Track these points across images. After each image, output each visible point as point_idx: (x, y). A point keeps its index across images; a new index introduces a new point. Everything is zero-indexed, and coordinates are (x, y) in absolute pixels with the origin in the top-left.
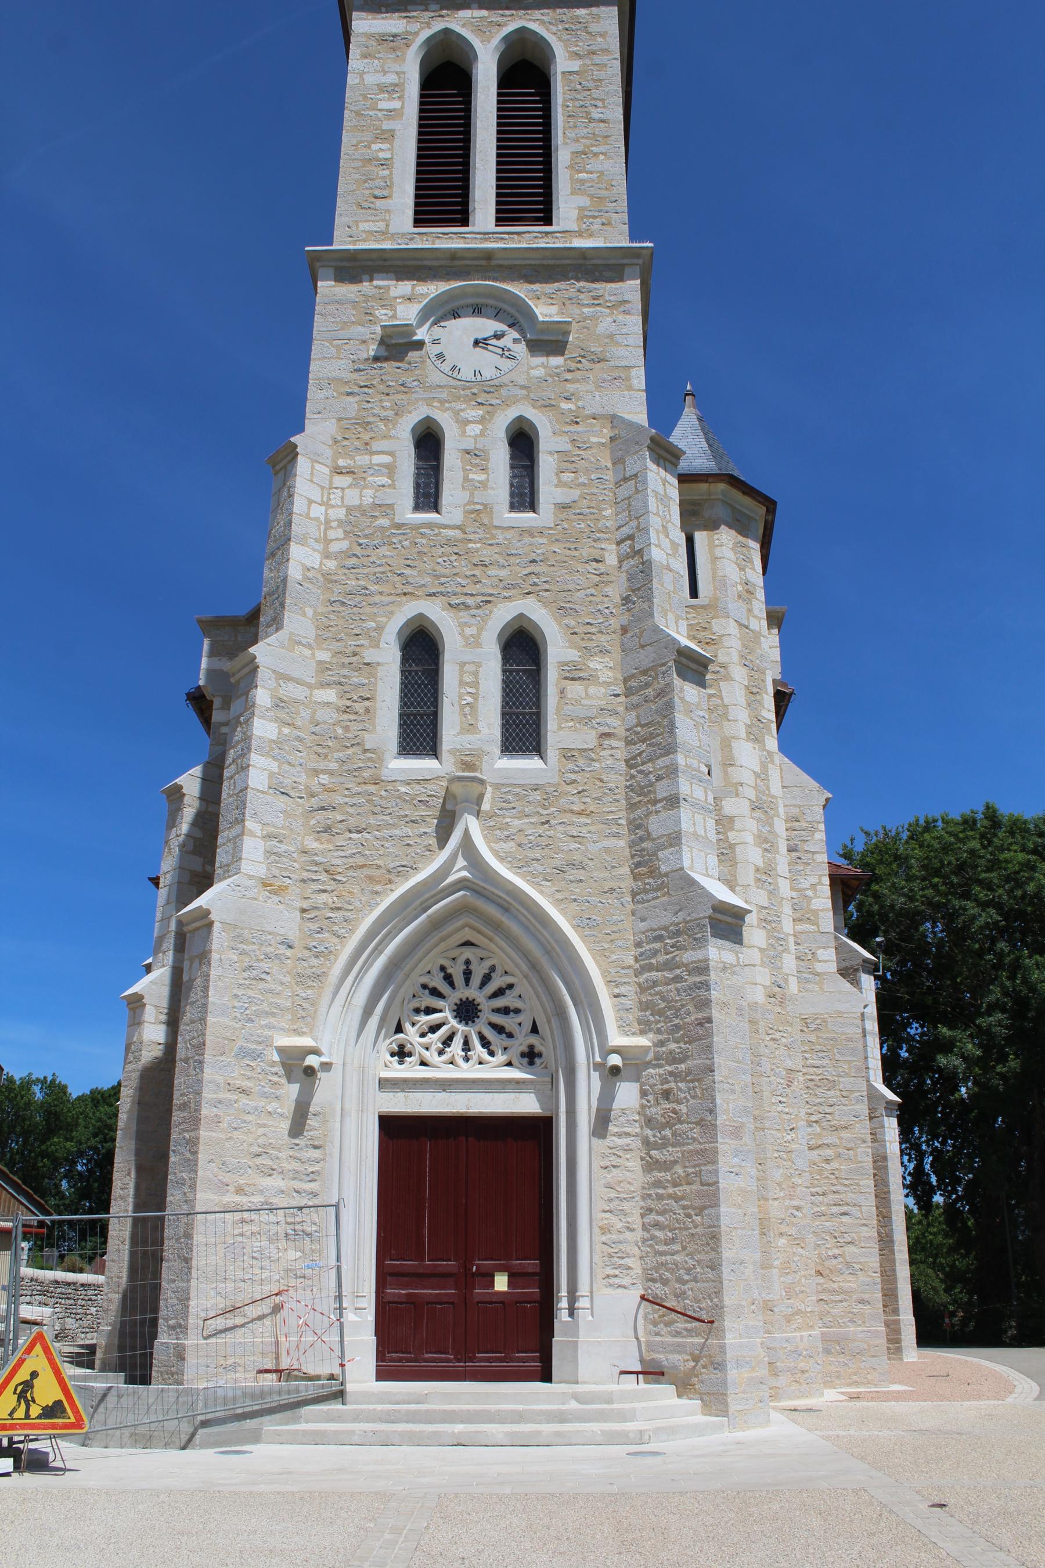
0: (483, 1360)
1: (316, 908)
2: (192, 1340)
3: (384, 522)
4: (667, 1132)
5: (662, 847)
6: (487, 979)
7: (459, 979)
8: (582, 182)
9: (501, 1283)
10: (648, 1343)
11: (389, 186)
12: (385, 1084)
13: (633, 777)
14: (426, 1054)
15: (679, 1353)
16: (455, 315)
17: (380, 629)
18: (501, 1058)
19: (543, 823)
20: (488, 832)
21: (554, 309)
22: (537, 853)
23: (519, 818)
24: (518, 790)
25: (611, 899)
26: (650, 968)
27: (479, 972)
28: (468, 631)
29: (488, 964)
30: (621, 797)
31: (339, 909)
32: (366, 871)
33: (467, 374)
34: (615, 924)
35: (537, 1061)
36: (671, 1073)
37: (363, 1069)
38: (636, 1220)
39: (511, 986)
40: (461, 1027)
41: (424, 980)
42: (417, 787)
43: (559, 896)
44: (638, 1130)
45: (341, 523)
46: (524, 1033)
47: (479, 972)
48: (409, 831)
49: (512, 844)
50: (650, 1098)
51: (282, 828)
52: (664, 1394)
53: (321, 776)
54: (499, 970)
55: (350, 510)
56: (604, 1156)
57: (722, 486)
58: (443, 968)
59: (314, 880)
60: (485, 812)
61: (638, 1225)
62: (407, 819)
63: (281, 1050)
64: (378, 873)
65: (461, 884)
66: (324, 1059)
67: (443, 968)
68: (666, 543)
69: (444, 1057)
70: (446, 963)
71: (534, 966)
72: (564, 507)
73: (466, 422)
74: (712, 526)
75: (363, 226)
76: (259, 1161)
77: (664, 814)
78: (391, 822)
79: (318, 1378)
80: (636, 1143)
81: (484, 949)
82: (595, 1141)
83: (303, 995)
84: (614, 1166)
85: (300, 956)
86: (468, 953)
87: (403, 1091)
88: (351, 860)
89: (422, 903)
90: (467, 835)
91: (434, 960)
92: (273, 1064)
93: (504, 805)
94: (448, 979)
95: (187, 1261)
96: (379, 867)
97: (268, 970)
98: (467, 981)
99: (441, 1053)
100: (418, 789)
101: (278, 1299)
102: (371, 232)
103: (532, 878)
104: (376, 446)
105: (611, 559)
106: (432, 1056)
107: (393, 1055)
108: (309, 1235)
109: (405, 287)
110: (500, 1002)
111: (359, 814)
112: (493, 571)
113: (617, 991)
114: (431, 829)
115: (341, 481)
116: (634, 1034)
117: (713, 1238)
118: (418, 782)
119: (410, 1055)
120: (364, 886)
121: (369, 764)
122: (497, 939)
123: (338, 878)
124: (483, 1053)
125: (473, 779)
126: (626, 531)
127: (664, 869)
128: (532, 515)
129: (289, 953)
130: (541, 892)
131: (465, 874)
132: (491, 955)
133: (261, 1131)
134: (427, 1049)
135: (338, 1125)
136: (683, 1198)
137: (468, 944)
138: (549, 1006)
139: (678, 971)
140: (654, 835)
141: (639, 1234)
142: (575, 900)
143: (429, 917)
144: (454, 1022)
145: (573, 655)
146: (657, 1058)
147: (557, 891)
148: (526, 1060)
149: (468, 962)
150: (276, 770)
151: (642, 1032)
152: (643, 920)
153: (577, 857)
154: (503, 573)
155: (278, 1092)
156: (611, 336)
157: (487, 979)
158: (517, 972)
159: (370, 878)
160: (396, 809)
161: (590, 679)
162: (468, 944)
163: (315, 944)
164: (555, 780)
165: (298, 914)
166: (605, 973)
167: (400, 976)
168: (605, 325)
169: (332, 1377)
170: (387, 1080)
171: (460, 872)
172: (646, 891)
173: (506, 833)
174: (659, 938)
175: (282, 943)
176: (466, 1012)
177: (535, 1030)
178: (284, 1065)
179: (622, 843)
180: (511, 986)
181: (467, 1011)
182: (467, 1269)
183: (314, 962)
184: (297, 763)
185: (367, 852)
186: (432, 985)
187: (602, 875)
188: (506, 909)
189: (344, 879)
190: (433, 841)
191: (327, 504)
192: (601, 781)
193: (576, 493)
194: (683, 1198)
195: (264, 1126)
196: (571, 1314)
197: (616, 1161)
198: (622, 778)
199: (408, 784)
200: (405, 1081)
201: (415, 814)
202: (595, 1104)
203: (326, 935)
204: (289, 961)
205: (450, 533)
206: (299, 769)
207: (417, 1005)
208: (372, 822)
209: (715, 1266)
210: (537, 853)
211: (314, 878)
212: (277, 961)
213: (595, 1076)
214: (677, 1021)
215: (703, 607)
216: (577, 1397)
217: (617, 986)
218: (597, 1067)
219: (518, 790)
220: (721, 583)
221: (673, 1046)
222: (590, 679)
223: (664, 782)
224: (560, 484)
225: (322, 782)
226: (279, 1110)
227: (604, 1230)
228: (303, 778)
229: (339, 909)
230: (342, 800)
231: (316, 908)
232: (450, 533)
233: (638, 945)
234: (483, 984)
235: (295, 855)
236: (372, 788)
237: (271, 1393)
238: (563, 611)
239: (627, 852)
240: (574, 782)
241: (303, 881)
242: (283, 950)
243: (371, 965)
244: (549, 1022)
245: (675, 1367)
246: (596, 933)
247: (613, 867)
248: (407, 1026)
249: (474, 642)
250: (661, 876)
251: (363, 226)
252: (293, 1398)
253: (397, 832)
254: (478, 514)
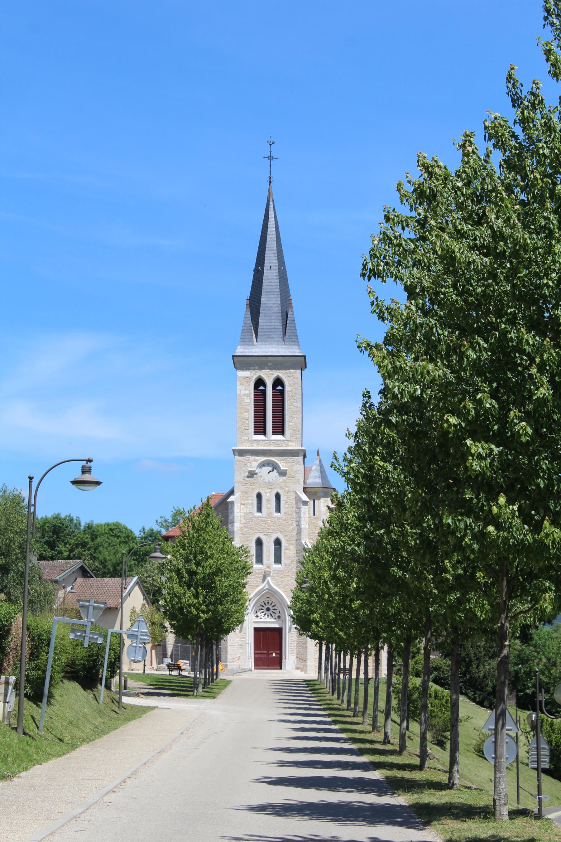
0: (271, 667)
2: (228, 663)
3: (251, 516)
6: (271, 604)
7: (267, 604)
8: (291, 426)
9: (274, 655)
11: (248, 426)
12: (255, 622)
16: (264, 466)
17: (252, 539)
20: (272, 579)
21: (284, 464)
27: (270, 602)
28: (268, 540)
33: (266, 481)
37: (251, 620)
38: (295, 645)
45: (243, 516)
47: (270, 602)
52: (299, 671)
55: (245, 513)
57: (321, 489)
65: (267, 589)
68: (305, 522)
71: (280, 603)
72: (285, 513)
73: (267, 493)
74: (319, 499)
75: (244, 438)
86: (268, 599)
91: (262, 600)
94: (265, 604)
95: (227, 652)
100: (260, 571)
102: (245, 440)
103: (279, 588)
104: (249, 498)
105: (295, 525)
106: (262, 617)
109: (253, 458)
110: (274, 608)
112: (272, 527)
115: (243, 506)
117: (307, 648)
126: (297, 519)
128: (279, 514)
145: (287, 545)
154: (274, 528)
156: (296, 471)
157: (271, 604)
161: (290, 550)
168: (295, 468)
171: (267, 587)
176: (268, 609)
188: (275, 593)
191: (240, 512)
193: (288, 510)
201: (259, 576)
205: (264, 519)
209: (306, 652)
210: (280, 583)
215: (316, 518)
220: (320, 512)
222: (290, 550)
224: (285, 508)
232: (264, 519)
238: (286, 536)
249: (269, 542)
251: (244, 438)
254: (270, 514)
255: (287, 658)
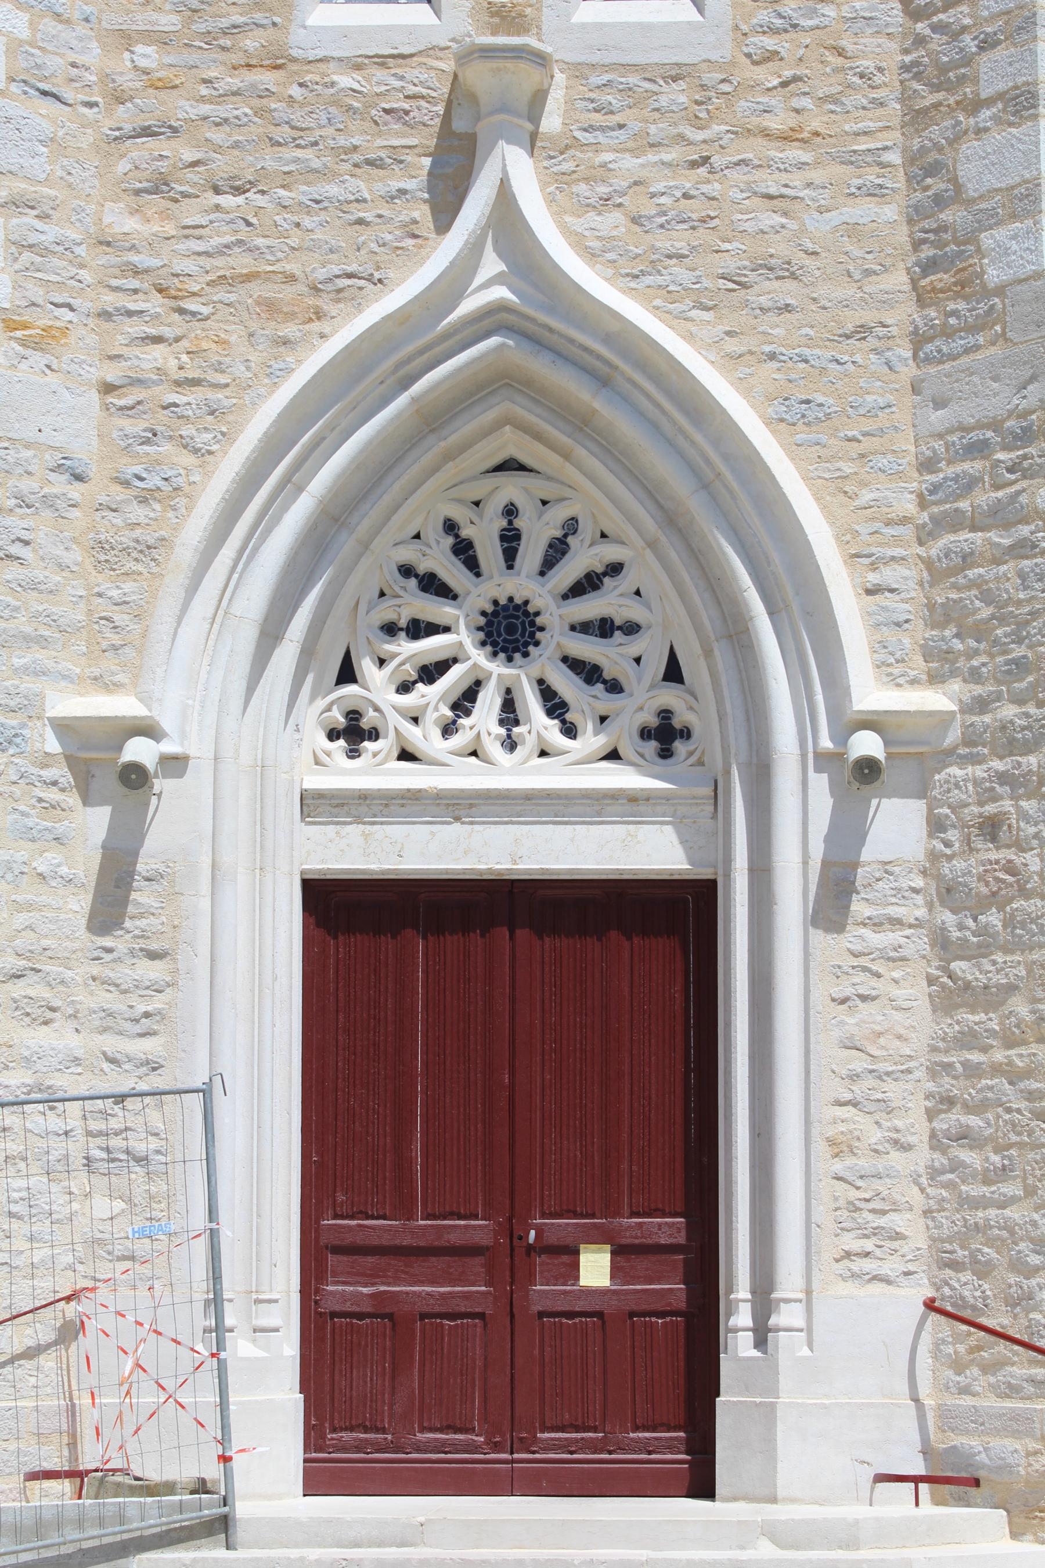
1: (140, 382)
4: (993, 918)
5: (990, 220)
7: (489, 552)
10: (944, 1413)
13: (920, 41)
14: (414, 735)
15: (1016, 1434)
18: (590, 741)
19: (694, 165)
22: (679, 240)
23: (635, 152)
24: (633, 80)
25: (860, 353)
26: (954, 522)
29: (559, 514)
30: (889, 94)
31: (195, 382)
32: (257, 289)
34: (870, 414)
35: (679, 746)
36: (1003, 778)
37: (262, 769)
39: (615, 569)
40: (496, 669)
41: (407, 554)
42: (380, 74)
43: (733, 346)
44: (921, 912)
46: (647, 681)
48: (359, 186)
49: (616, 217)
50: (952, 835)
51: (46, 182)
53: (140, 49)
54: (587, 530)
56: (839, 973)
58: (450, 527)
59: (130, 314)
60: (551, 138)
61: (919, 1136)
62: (357, 158)
63: (64, 727)
64: (287, 293)
66: (168, 747)
67: (450, 527)
69: (457, 741)
70: (459, 514)
76: (18, 989)
77: (997, 137)
78: (316, 164)
79: (169, 1488)
80: (919, 944)
81: (550, 478)
82: (818, 936)
83: (114, 593)
84: (864, 998)
85: (103, 499)
87: (358, 820)
88: (219, 262)
89: (399, 365)
90: (505, 195)
92: (46, 760)
93: (597, 119)
96: (291, 278)
97: (26, 535)
98: (510, 556)
99: (448, 730)
101: (71, 1310)
107: (333, 735)
108: (142, 1160)
110: (589, 608)
111: (236, 145)
113: (873, 578)
114: (416, 183)
116: (914, 682)
118: (382, 61)
119: (374, 734)
120: (254, 326)
121: (258, 17)
122: (581, 453)
123: (191, 305)
124: (550, 729)
125: (519, 53)
127: (994, 275)
129: (76, 492)
130: (689, 337)
131: (501, 293)
132: (567, 492)
133: (21, 919)
134: (415, 720)
135: (205, 904)
136: (1028, 1073)
137: (510, 466)
138: (707, 617)
139: (1025, 530)
140: (971, 190)
141: (923, 1156)
142: (772, 356)
143: (414, 400)
144: (478, 657)
146: (968, 741)
147: (728, 333)
148: (653, 745)
149: (511, 511)
150: (25, 34)
151: (935, 679)
152: (939, 404)
153: (779, 248)
155: (61, 828)
158: (631, 533)
159: (270, 307)
160: (330, 131)
162: (510, 466)
163: (138, 469)
164: (724, 51)
165: (94, 396)
166: (844, 536)
167: (346, 545)
169: (202, 1487)
170: (320, 795)
172: (948, 333)
173: (603, 190)
174: (979, 449)
175: (58, 469)
177: (673, 673)
178: (71, 761)
179: (890, 212)
180: (615, 569)
181: (511, 629)
182: (513, 1234)
183: (138, 513)
184: (77, 15)
185: (260, 242)
186: (423, 567)
187: (839, 294)
189: (205, 310)
190: (422, 213)
192: (840, 52)
194: (1028, 1073)
195: (29, 907)
196: (761, 1342)
197: (867, 985)
198: (893, 46)
199: (358, 67)
200: (364, 797)
201: (375, 146)
202: (817, 850)
203: (166, 448)
204: (75, 513)
206: (82, 30)
207: (390, 616)
208: (270, 164)
210: (679, 240)
211: (132, 306)
212: (48, 514)
213: (820, 783)
214: (1019, 651)
216: (773, 1533)
217: (873, 567)
218: (825, 761)
219: (633, 80)
221: (1009, 711)
223: (1000, 54)
225: (143, 63)
226: (64, 870)
227: (839, 1147)
228: (93, 55)
229: (195, 382)
230: (188, 109)
231: (140, 382)
233: (927, 465)
234: (548, 564)
235: (80, 251)
236: (267, 79)
237: (59, 1523)
239: (902, 235)
240: (772, 56)
241: (105, 315)
242: (60, 484)
243: (277, 520)
244: (708, 653)
245: (1005, 1468)
246: (823, 438)
247: (868, 273)
248: (366, 666)
250: (987, 293)
252: (112, 1534)
253: (333, 190)
255: (786, 1316)
